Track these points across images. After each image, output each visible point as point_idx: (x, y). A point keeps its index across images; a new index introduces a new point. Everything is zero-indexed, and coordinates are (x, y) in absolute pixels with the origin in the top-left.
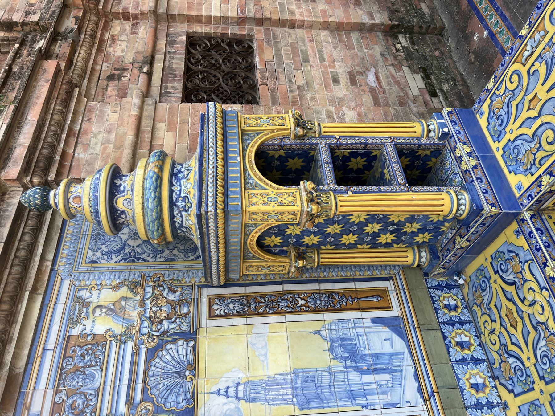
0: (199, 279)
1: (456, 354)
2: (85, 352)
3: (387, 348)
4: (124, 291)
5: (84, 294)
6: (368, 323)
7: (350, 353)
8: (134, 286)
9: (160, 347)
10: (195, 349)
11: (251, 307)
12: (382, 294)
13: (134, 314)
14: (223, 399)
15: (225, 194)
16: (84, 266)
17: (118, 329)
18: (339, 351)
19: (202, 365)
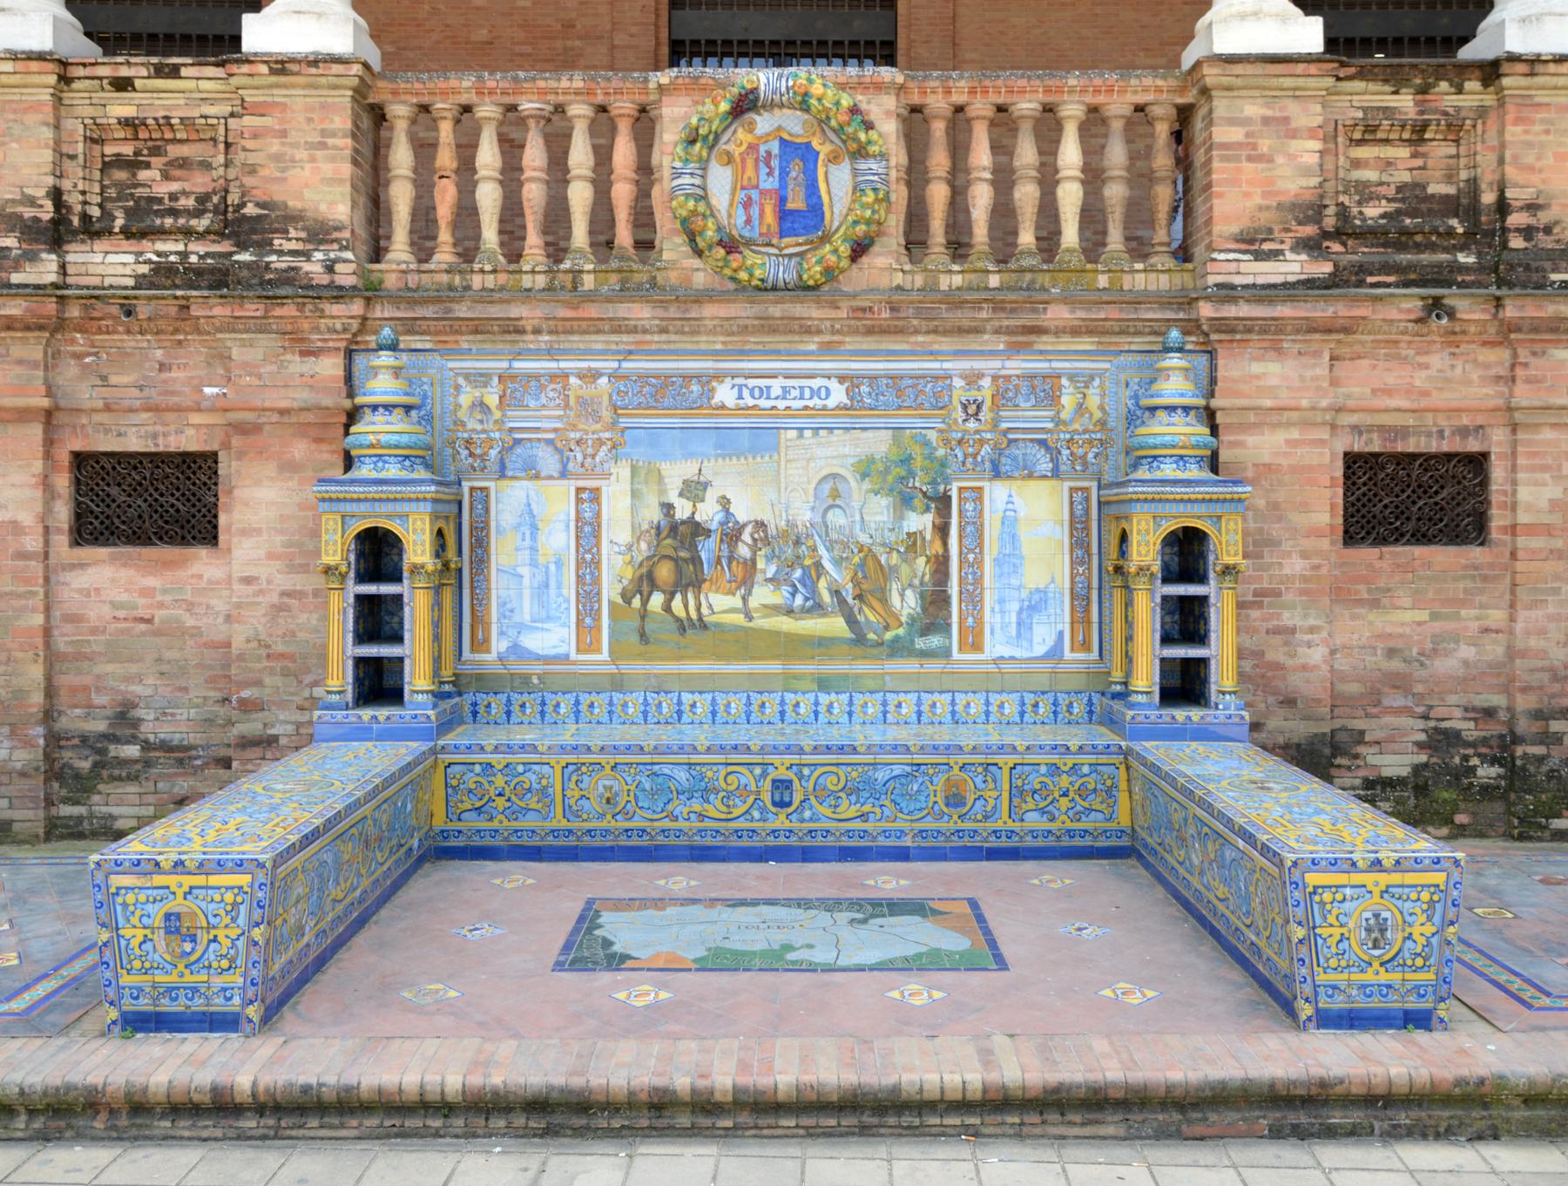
0: (1107, 478)
1: (1030, 699)
2: (1046, 390)
3: (1037, 639)
4: (1098, 415)
5: (1097, 382)
6: (1060, 627)
7: (1034, 606)
8: (1102, 423)
9: (1048, 448)
10: (1045, 477)
11: (1078, 525)
12: (1086, 646)
13: (1076, 426)
14: (1005, 499)
15: (1146, 500)
16: (1123, 377)
17: (1064, 415)
18: (1036, 597)
19: (1032, 483)
